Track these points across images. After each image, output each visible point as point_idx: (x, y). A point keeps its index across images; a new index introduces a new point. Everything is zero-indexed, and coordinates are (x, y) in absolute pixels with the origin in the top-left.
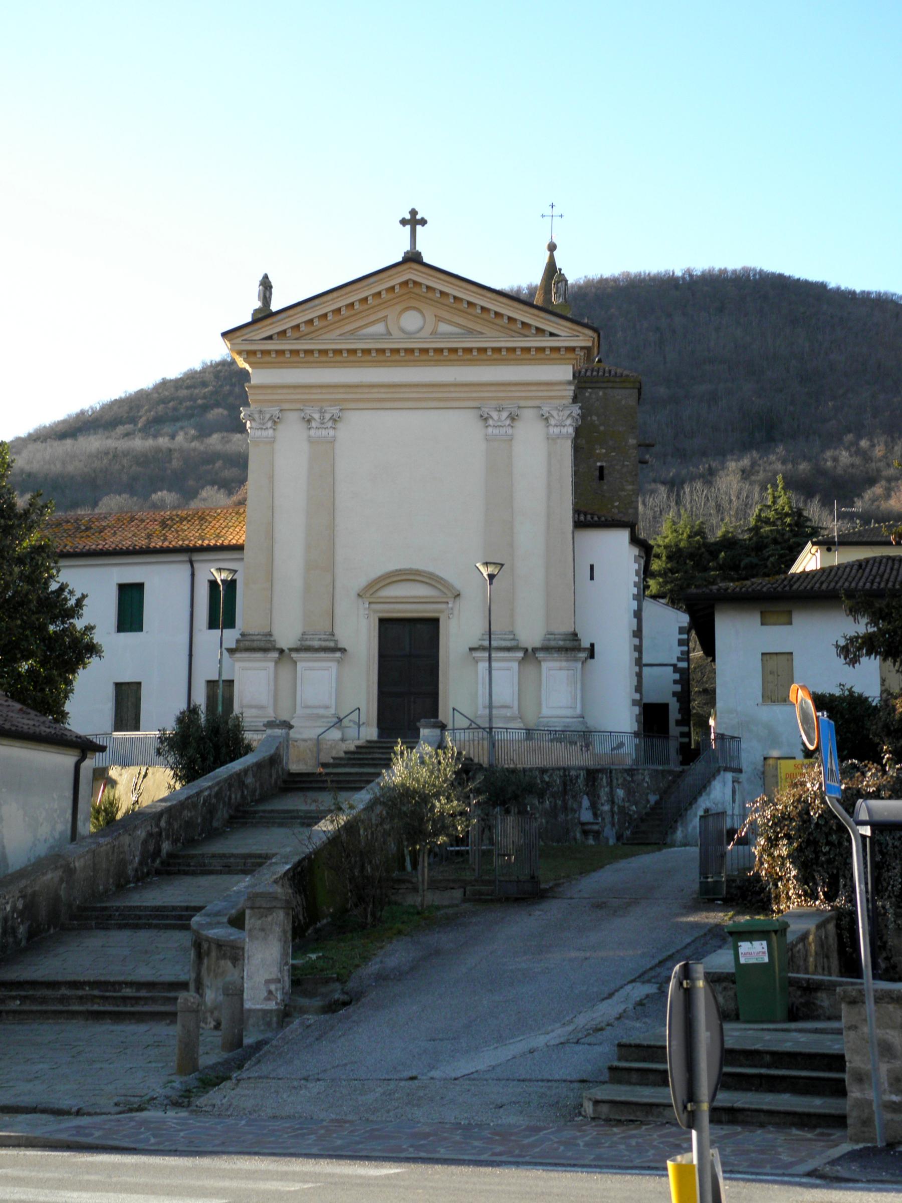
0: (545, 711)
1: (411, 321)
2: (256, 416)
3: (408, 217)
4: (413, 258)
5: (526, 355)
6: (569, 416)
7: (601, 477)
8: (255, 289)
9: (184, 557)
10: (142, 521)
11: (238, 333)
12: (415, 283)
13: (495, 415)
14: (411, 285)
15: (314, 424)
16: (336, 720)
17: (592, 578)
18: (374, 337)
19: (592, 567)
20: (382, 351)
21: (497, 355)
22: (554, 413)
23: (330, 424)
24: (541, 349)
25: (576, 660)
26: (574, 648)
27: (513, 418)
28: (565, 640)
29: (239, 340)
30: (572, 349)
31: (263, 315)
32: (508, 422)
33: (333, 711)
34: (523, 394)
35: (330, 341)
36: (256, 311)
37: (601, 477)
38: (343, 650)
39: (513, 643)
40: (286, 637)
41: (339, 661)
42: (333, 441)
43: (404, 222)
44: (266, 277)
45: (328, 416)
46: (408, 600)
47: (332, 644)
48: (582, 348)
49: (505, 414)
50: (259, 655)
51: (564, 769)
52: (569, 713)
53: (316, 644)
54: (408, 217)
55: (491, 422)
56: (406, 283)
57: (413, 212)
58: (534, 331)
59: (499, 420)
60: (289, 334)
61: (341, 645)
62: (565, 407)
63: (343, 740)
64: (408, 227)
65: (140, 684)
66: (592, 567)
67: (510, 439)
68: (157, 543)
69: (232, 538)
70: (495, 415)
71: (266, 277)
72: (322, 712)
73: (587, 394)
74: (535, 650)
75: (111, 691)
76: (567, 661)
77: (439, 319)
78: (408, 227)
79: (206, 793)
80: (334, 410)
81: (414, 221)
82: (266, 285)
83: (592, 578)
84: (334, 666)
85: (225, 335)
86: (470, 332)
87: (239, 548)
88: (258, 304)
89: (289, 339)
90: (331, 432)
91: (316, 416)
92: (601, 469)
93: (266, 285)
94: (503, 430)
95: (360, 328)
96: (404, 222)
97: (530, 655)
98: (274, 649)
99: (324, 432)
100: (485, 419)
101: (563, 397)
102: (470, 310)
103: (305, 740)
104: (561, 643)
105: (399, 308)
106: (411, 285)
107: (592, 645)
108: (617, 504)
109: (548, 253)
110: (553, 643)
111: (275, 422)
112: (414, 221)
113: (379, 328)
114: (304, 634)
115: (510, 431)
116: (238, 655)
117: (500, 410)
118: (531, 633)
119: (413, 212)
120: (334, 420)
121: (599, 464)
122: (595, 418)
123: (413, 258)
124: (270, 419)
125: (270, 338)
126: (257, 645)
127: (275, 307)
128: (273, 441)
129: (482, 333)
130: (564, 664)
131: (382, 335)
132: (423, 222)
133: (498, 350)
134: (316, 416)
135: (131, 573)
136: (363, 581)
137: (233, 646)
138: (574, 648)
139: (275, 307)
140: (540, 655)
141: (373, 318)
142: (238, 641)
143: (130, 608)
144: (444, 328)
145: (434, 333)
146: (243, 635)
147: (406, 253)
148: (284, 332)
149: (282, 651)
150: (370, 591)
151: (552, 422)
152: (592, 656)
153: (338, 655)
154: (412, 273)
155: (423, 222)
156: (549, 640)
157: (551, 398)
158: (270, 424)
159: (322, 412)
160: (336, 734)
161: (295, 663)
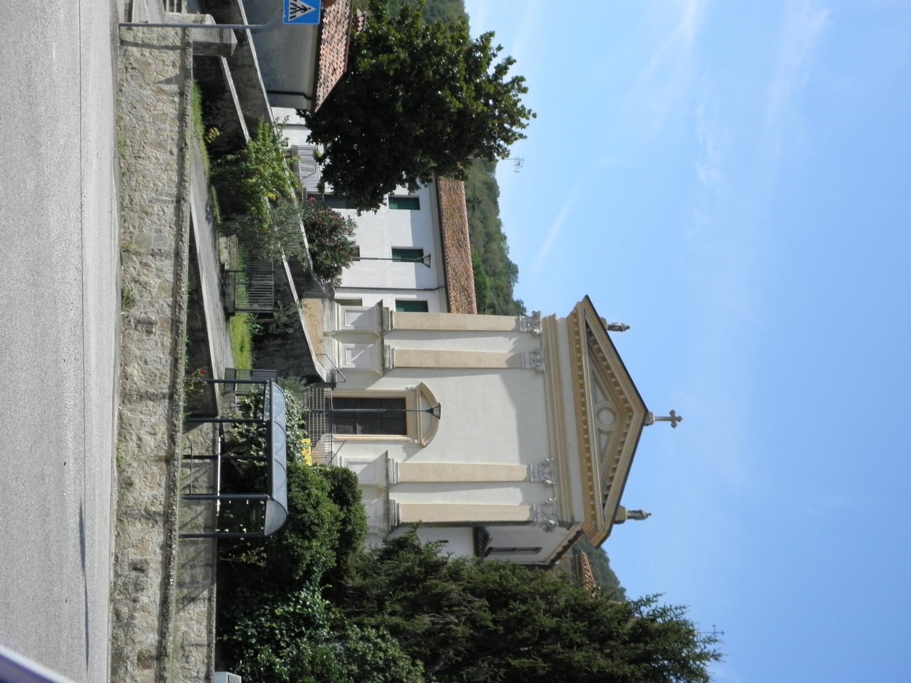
3: (677, 415)
9: (443, 284)
15: (532, 356)
19: (446, 541)
24: (592, 498)
30: (594, 517)
43: (672, 413)
48: (596, 526)
54: (677, 415)
56: (630, 410)
57: (679, 419)
59: (543, 473)
66: (446, 541)
81: (674, 419)
82: (621, 329)
85: (587, 297)
89: (588, 338)
91: (538, 357)
93: (621, 329)
95: (601, 389)
96: (672, 413)
99: (528, 361)
105: (614, 408)
112: (674, 419)
119: (679, 419)
120: (536, 371)
125: (587, 326)
127: (611, 333)
132: (674, 425)
134: (538, 357)
137: (384, 305)
139: (611, 333)
142: (388, 308)
150: (423, 392)
154: (637, 416)
155: (674, 425)
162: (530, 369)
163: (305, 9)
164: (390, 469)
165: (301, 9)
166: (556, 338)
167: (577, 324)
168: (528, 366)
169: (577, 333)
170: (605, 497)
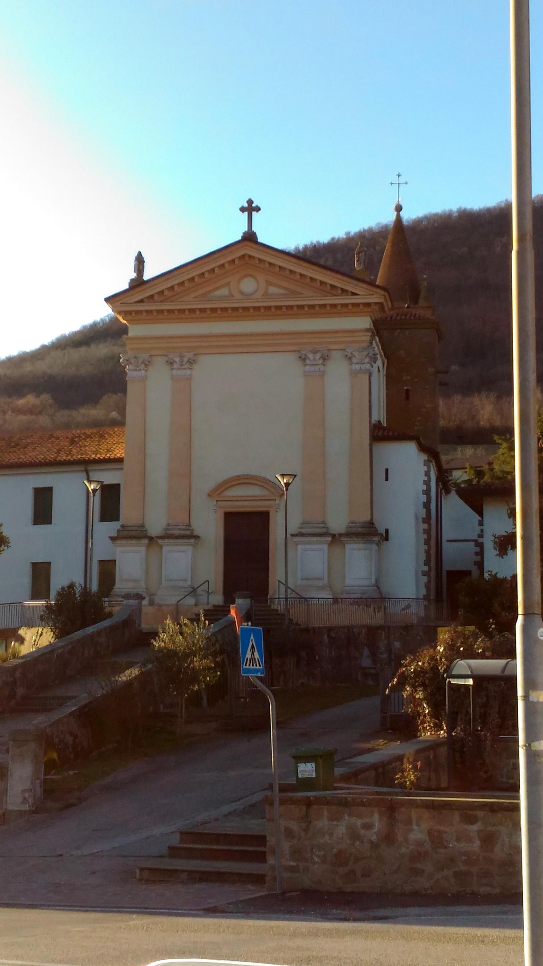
0: (348, 582)
1: (248, 285)
2: (132, 361)
3: (246, 205)
4: (250, 237)
5: (333, 310)
6: (367, 356)
7: (407, 398)
8: (132, 263)
9: (82, 468)
10: (58, 438)
11: (117, 298)
12: (250, 256)
13: (311, 356)
14: (247, 258)
15: (175, 366)
16: (191, 590)
17: (387, 479)
18: (220, 299)
19: (387, 470)
20: (225, 310)
21: (312, 311)
22: (356, 354)
23: (187, 366)
25: (371, 542)
26: (371, 533)
27: (325, 358)
28: (362, 527)
29: (118, 304)
30: (368, 305)
31: (138, 283)
32: (321, 361)
33: (189, 583)
34: (332, 340)
35: (188, 302)
36: (132, 280)
37: (407, 398)
38: (197, 537)
39: (324, 530)
40: (155, 528)
41: (194, 546)
42: (189, 379)
43: (243, 209)
44: (140, 254)
45: (186, 360)
46: (245, 498)
47: (188, 533)
48: (376, 304)
49: (318, 356)
50: (134, 542)
51: (348, 627)
52: (366, 582)
53: (177, 532)
54: (246, 205)
55: (308, 362)
56: (243, 257)
57: (250, 202)
58: (340, 292)
59: (314, 360)
60: (156, 298)
61: (195, 534)
62: (364, 349)
63: (196, 605)
64: (246, 213)
65: (49, 563)
66: (387, 470)
67: (322, 374)
68: (63, 457)
69: (118, 453)
70: (311, 356)
71: (140, 254)
72: (181, 584)
73: (396, 334)
74: (340, 535)
75: (28, 569)
76: (365, 543)
77: (269, 283)
78: (246, 213)
79: (60, 651)
80: (189, 355)
81: (250, 209)
82: (140, 261)
83: (387, 479)
84: (190, 548)
85: (107, 300)
86: (293, 293)
87: (120, 460)
88: (134, 275)
90: (188, 372)
91: (177, 360)
92: (407, 391)
93: (140, 261)
94: (317, 368)
95: (211, 291)
96: (243, 209)
97: (336, 539)
98: (146, 537)
99: (182, 372)
100: (303, 359)
101: (363, 341)
102: (292, 276)
103: (168, 606)
104: (360, 529)
106: (247, 258)
107: (387, 531)
108: (419, 418)
109: (396, 213)
110: (354, 530)
111: (146, 365)
112: (250, 209)
113: (224, 292)
114: (168, 525)
115: (322, 368)
116: (118, 542)
117: (315, 352)
118: (338, 523)
119: (250, 202)
120: (191, 362)
121: (405, 388)
122: (402, 352)
123: (250, 237)
124: (143, 362)
125: (142, 301)
126: (134, 534)
127: (147, 276)
128: (144, 379)
129: (301, 294)
130: (362, 546)
131: (227, 296)
132: (258, 209)
133: (312, 307)
134: (177, 360)
135: (43, 480)
136: (212, 484)
137: (115, 534)
138: (371, 533)
139: (147, 276)
140: (344, 539)
141: (219, 284)
142: (118, 531)
143: (43, 508)
144: (272, 290)
145: (266, 294)
146: (122, 526)
147: (244, 233)
148: (151, 297)
149: (151, 539)
151: (354, 360)
152: (387, 539)
153: (192, 541)
155: (258, 209)
156: (351, 527)
157: (353, 342)
158: (142, 366)
159: (181, 357)
160: (190, 601)
161: (161, 547)
162: (146, 370)
163: (253, 647)
164: (310, 531)
165: (253, 653)
166: (181, 337)
167: (138, 312)
168: (143, 372)
169: (149, 312)
170: (344, 291)
